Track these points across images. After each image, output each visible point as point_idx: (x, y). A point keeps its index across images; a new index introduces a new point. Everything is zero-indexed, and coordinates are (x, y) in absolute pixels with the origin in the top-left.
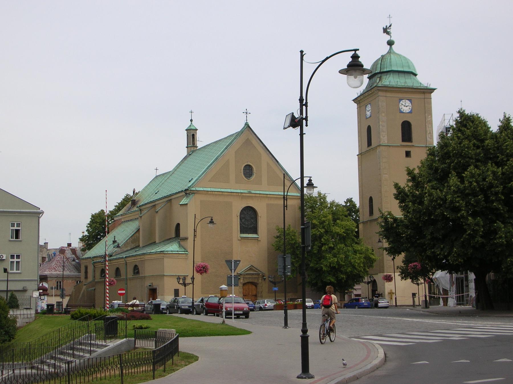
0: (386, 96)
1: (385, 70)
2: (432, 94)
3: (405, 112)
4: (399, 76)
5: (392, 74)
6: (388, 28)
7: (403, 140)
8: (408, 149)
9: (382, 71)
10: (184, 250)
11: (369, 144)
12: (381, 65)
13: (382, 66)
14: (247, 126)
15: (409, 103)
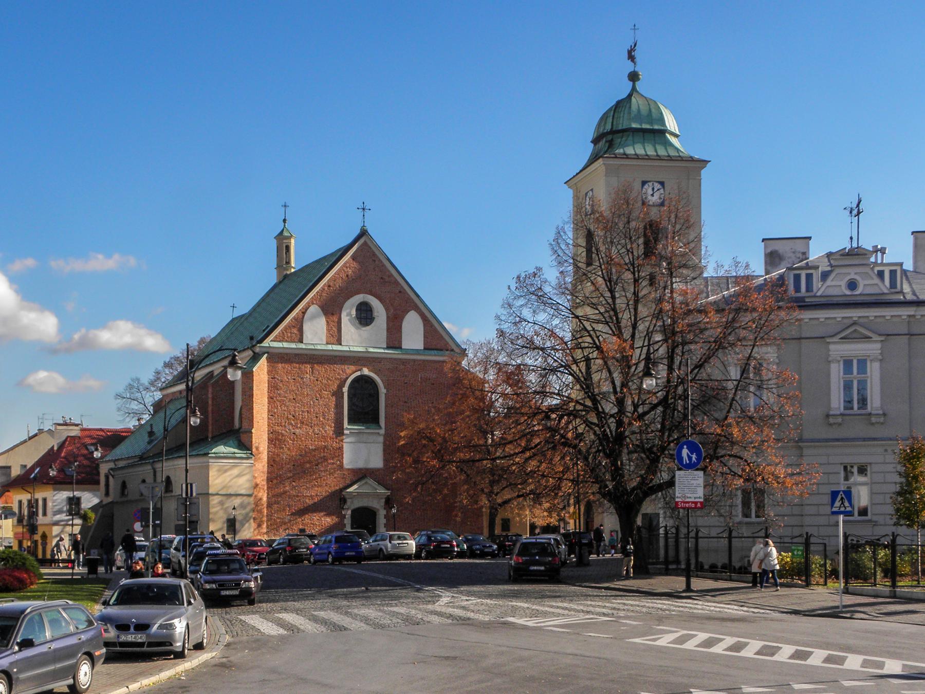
1: (620, 128)
4: (644, 139)
5: (630, 138)
9: (614, 129)
12: (613, 118)
14: (363, 233)
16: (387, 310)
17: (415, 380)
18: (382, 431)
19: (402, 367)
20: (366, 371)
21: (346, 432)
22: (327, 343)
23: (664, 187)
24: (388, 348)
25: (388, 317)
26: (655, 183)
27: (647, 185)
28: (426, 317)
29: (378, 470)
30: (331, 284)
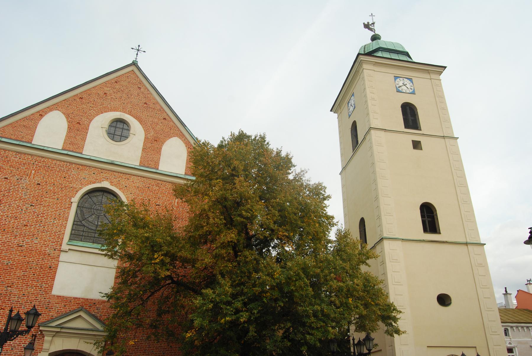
0: (374, 71)
2: (442, 77)
3: (405, 92)
6: (371, 25)
7: (407, 126)
8: (417, 138)
11: (355, 143)
13: (365, 49)
14: (134, 64)
15: (410, 82)
16: (146, 131)
19: (155, 188)
20: (106, 184)
21: (64, 247)
22: (63, 149)
23: (412, 83)
24: (140, 165)
25: (146, 138)
26: (404, 79)
27: (398, 79)
30: (84, 96)
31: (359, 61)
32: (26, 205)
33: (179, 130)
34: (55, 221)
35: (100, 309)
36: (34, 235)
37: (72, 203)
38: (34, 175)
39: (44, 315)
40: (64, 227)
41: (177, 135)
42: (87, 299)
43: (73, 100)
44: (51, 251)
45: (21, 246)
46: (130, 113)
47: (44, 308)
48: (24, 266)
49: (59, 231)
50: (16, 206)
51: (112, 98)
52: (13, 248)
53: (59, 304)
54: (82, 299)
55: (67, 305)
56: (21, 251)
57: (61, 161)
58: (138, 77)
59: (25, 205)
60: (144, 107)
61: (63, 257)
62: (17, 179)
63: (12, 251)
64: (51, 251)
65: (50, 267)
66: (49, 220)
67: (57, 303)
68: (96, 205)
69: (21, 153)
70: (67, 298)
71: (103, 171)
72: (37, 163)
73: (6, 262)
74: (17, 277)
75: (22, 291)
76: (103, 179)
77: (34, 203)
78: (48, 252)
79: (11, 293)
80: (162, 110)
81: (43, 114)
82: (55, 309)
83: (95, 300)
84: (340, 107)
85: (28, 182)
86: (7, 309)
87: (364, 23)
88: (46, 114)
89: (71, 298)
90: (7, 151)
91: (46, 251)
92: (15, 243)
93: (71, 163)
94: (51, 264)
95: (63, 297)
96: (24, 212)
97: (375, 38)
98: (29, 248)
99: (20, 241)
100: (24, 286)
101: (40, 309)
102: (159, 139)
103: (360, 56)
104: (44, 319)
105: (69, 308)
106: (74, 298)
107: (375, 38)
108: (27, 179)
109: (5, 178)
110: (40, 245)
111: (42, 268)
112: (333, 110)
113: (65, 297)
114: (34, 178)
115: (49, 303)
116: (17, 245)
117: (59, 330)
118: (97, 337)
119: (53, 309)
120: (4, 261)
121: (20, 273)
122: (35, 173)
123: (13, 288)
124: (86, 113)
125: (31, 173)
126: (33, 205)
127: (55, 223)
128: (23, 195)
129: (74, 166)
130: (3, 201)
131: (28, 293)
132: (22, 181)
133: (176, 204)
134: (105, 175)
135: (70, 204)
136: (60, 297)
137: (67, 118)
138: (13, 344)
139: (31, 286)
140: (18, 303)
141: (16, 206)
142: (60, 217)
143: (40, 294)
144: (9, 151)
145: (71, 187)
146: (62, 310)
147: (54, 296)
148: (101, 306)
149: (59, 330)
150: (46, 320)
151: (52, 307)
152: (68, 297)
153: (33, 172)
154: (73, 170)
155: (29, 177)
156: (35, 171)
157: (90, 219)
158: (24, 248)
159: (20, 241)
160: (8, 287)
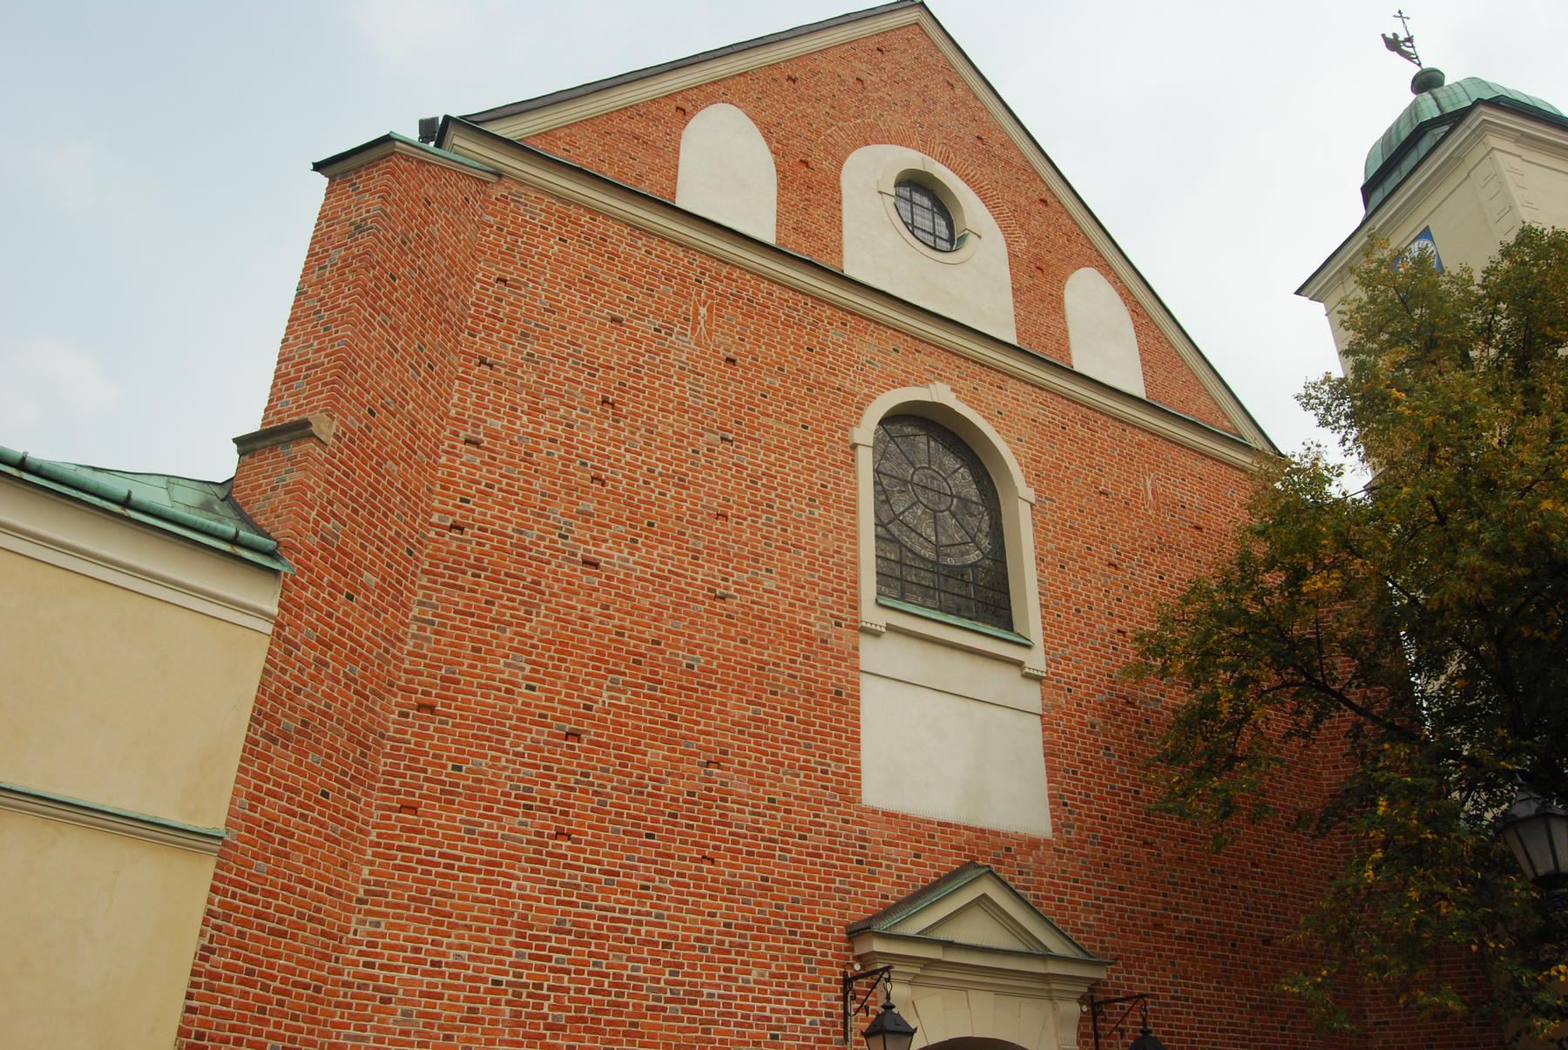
10: (230, 528)
16: (1005, 229)
17: (1136, 493)
18: (1036, 660)
19: (1083, 432)
20: (940, 393)
21: (872, 615)
25: (1012, 256)
28: (1138, 303)
29: (1034, 844)
31: (1472, 123)
32: (707, 435)
33: (1092, 246)
34: (817, 512)
35: (1028, 874)
36: (756, 557)
37: (854, 446)
38: (708, 322)
39: (856, 893)
40: (848, 536)
41: (1090, 263)
42: (983, 831)
43: (769, 80)
44: (826, 628)
45: (723, 598)
46: (945, 161)
47: (850, 861)
48: (748, 680)
49: (836, 552)
50: (670, 433)
51: (882, 99)
52: (695, 601)
53: (897, 845)
54: (967, 828)
55: (924, 850)
56: (729, 616)
57: (784, 286)
58: (938, 50)
59: (702, 435)
60: (980, 152)
61: (872, 654)
62: (656, 330)
63: (698, 616)
64: (826, 628)
65: (838, 693)
66: (793, 502)
67: (890, 844)
68: (929, 468)
69: (648, 233)
70: (919, 822)
71: (921, 346)
72: (707, 279)
73: (683, 657)
74: (734, 723)
75: (763, 784)
76: (927, 375)
77: (731, 432)
78: (817, 628)
79: (725, 794)
80: (1027, 167)
81: (688, 107)
82: (888, 867)
83: (1006, 835)
84: (1342, 278)
85: (693, 346)
86: (722, 861)
87: (1383, 36)
88: (697, 108)
89: (929, 822)
90: (601, 218)
91: (810, 624)
92: (699, 583)
93: (819, 300)
94: (839, 680)
95: (905, 817)
96: (703, 462)
97: (1426, 82)
98: (752, 609)
99: (714, 576)
100: (764, 763)
101: (838, 863)
102: (1048, 266)
103: (1482, 109)
104: (858, 909)
105: (933, 866)
106: (940, 824)
107: (1426, 82)
108: (689, 333)
109: (614, 320)
110: (787, 600)
111: (812, 695)
112: (1305, 292)
113: (912, 819)
114: (710, 333)
115: (866, 840)
116: (709, 590)
117: (935, 953)
118: (1054, 986)
119: (880, 865)
120: (678, 655)
121: (740, 710)
122: (710, 317)
123: (729, 769)
124: (819, 135)
125: (696, 313)
126: (731, 437)
127: (816, 516)
128: (687, 395)
129: (828, 313)
130: (625, 409)
131: (785, 794)
132: (673, 338)
133: (1150, 497)
134: (930, 361)
135: (849, 450)
136: (895, 816)
137: (767, 136)
138: (774, 1016)
139: (790, 766)
140: (759, 835)
141: (670, 433)
142: (827, 496)
143: (827, 803)
144: (606, 217)
145: (839, 389)
146: (910, 871)
147: (875, 812)
148: (1031, 859)
149: (935, 953)
150: (865, 910)
151: (877, 858)
152: (923, 821)
153: (703, 311)
154: (829, 327)
155: (694, 329)
156: (710, 310)
157: (908, 517)
158: (732, 605)
159: (714, 576)
160: (709, 763)
